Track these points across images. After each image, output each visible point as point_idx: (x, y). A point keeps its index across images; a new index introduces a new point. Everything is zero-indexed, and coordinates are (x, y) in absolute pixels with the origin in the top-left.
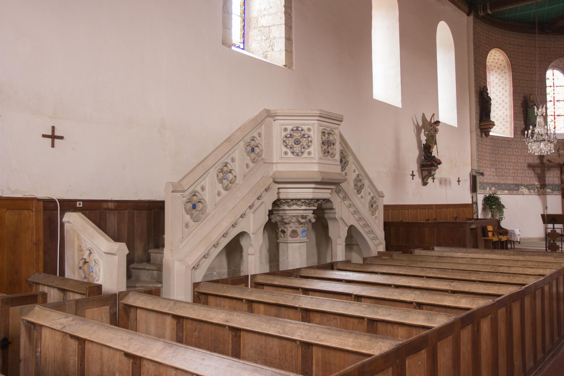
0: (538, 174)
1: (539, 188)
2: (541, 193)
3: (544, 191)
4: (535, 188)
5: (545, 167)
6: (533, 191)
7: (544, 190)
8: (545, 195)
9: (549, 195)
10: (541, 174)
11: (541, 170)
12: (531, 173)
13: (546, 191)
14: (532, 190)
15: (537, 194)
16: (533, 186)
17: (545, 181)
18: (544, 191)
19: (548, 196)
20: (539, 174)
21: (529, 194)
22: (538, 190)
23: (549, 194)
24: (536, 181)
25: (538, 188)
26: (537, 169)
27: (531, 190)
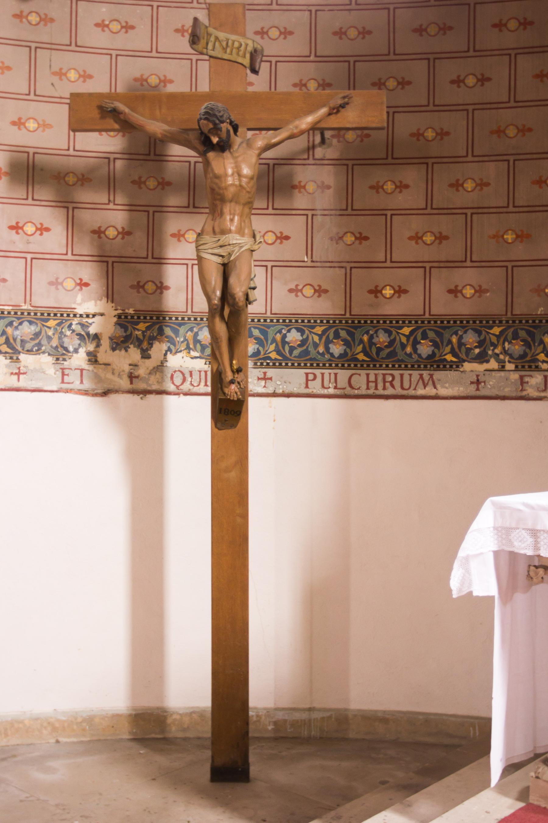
0: (98, 233)
1: (105, 343)
2: (125, 383)
3: (150, 364)
4: (71, 342)
5: (164, 184)
6: (46, 360)
7: (146, 355)
8: (151, 398)
9: (186, 394)
10: (125, 233)
11: (132, 208)
12: (42, 229)
13: (160, 368)
14: (38, 350)
15: (87, 385)
16: (52, 323)
17: (161, 288)
18: (150, 364)
19: (171, 401)
20: (111, 233)
21: (13, 381)
22: (93, 358)
23: (186, 387)
24: (82, 284)
25: (96, 337)
26: (102, 197)
27: (29, 351)
